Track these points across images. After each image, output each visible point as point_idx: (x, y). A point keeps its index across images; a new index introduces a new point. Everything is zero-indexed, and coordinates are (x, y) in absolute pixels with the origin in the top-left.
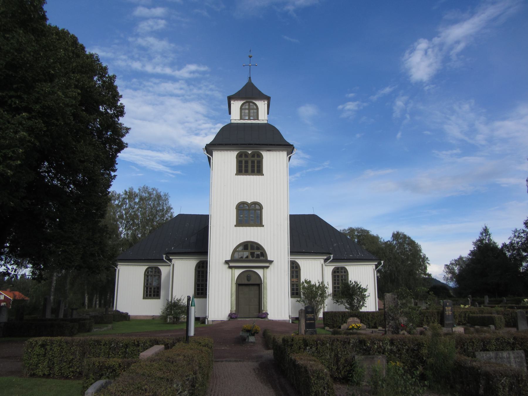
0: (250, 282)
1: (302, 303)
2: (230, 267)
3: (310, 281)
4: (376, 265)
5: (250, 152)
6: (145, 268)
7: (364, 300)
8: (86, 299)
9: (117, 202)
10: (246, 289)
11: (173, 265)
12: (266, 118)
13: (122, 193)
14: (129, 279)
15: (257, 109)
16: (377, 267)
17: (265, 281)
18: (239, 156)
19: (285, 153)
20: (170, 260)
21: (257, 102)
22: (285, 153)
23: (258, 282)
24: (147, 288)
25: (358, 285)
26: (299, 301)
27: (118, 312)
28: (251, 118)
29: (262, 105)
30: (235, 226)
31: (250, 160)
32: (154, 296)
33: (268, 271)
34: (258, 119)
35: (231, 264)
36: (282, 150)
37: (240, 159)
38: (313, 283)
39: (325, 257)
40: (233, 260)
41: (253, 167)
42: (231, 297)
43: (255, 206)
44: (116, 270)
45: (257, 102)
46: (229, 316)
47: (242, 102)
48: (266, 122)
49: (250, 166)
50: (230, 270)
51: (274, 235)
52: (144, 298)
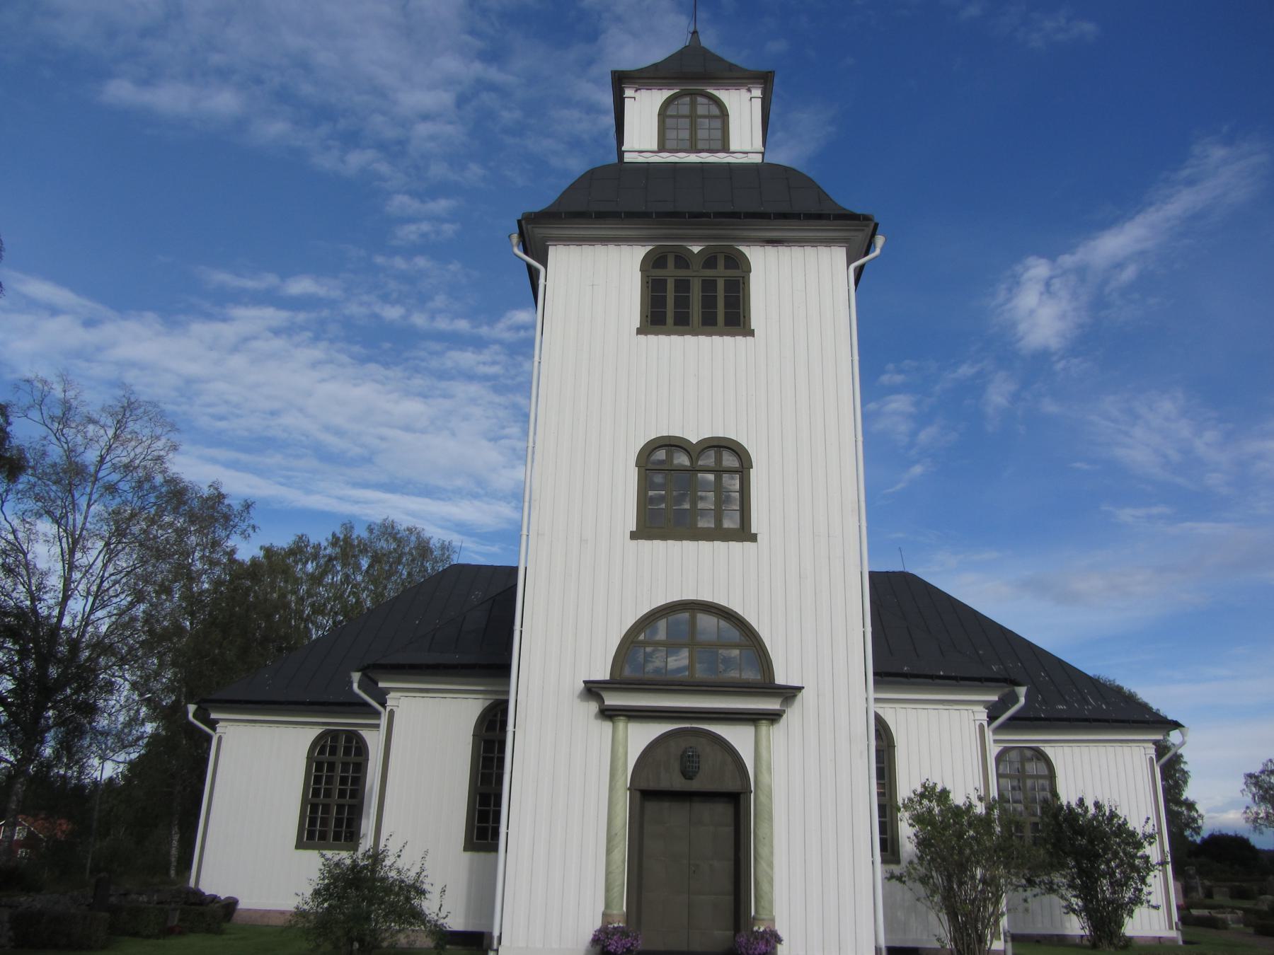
0: (695, 785)
1: (918, 886)
2: (608, 714)
3: (944, 794)
4: (1155, 742)
5: (696, 249)
6: (315, 732)
7: (1143, 880)
8: (175, 843)
9: (310, 567)
10: (675, 815)
11: (392, 713)
12: (758, 144)
13: (324, 544)
14: (257, 770)
15: (724, 114)
16: (1161, 749)
17: (764, 778)
18: (652, 264)
19: (839, 254)
20: (382, 698)
22: (839, 254)
23: (730, 786)
24: (314, 808)
25: (1113, 815)
26: (900, 879)
27: (197, 893)
28: (700, 146)
29: (743, 109)
30: (634, 536)
32: (337, 837)
33: (775, 734)
34: (725, 148)
35: (612, 700)
36: (828, 242)
37: (659, 273)
38: (958, 799)
39: (995, 698)
40: (617, 683)
41: (709, 302)
42: (609, 851)
43: (719, 459)
44: (209, 739)
46: (596, 940)
47: (666, 94)
48: (757, 159)
49: (695, 298)
50: (607, 726)
51: (801, 585)
52: (300, 845)
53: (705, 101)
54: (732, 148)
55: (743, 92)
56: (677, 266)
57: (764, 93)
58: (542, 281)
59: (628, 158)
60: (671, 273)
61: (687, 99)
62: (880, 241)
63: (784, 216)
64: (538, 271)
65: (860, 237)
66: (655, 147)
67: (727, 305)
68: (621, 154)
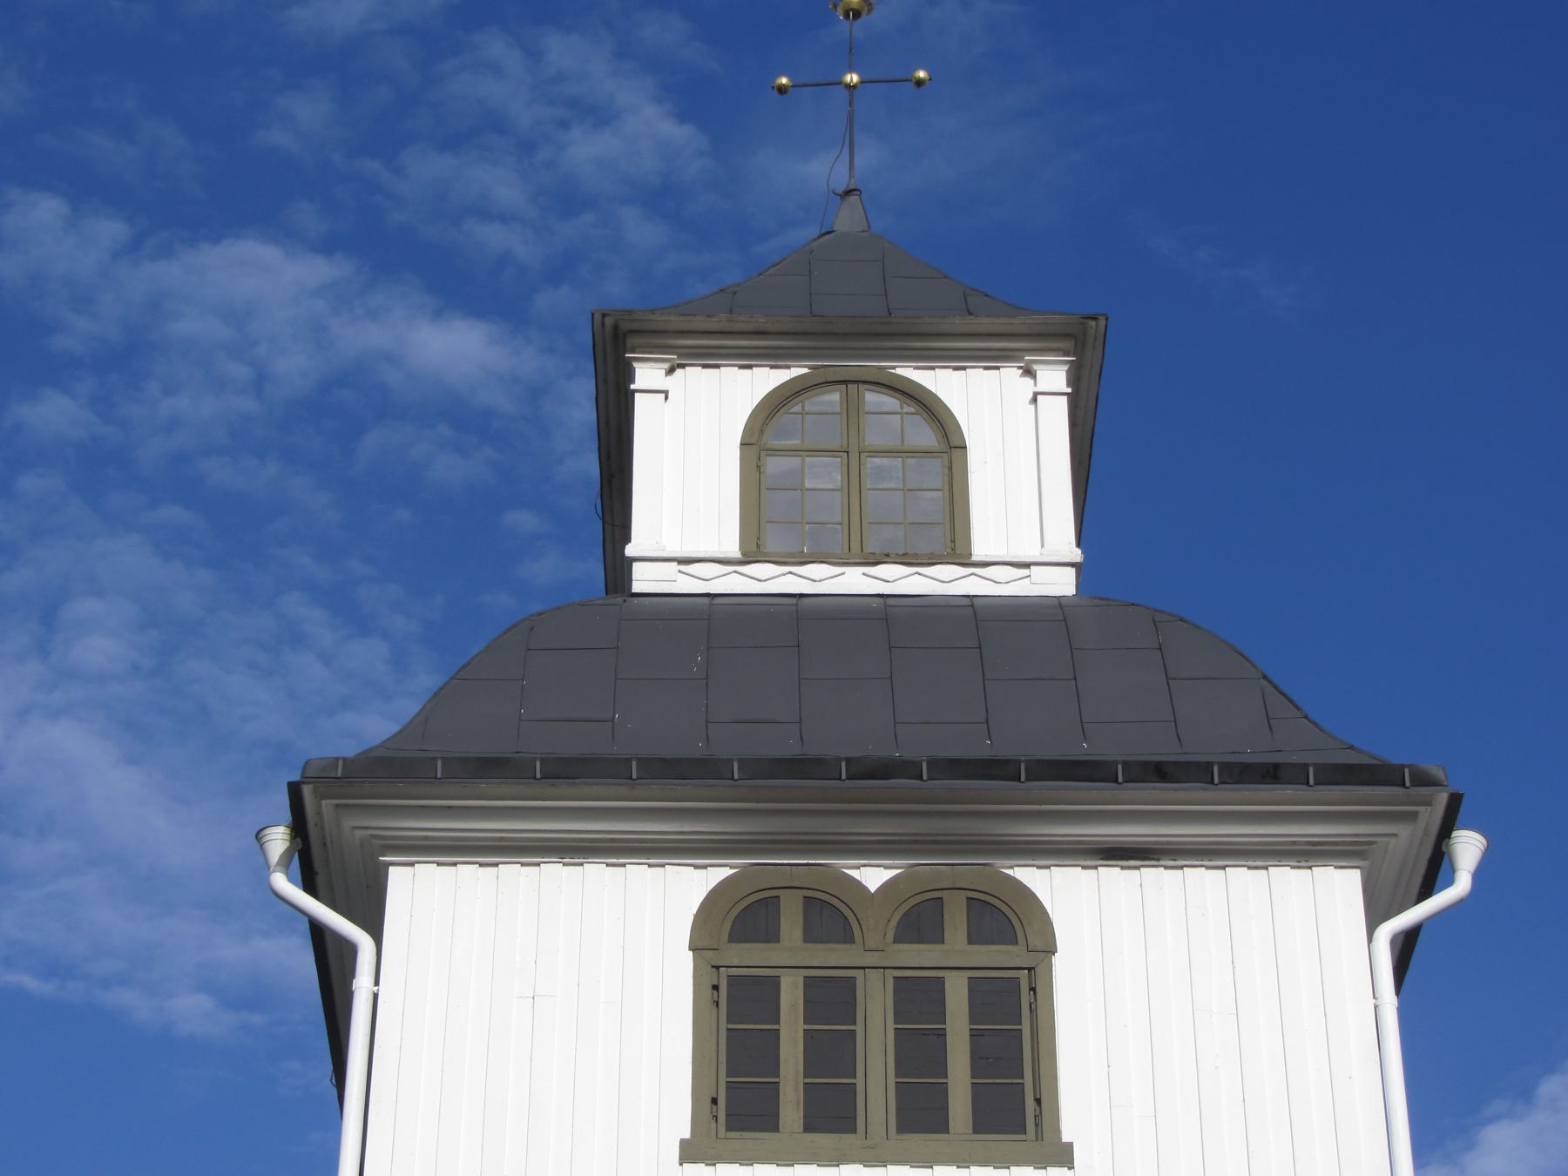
12: (1063, 540)
18: (729, 926)
19: (1342, 887)
21: (947, 384)
22: (1342, 887)
31: (875, 973)
34: (957, 552)
41: (919, 1052)
45: (947, 384)
47: (767, 379)
48: (1062, 584)
53: (889, 402)
54: (979, 551)
55: (1010, 374)
56: (809, 937)
57: (1074, 379)
58: (362, 984)
59: (645, 579)
60: (791, 956)
61: (833, 397)
62: (1468, 848)
63: (1160, 773)
64: (349, 950)
65: (1403, 841)
66: (733, 549)
67: (980, 1062)
68: (618, 570)
